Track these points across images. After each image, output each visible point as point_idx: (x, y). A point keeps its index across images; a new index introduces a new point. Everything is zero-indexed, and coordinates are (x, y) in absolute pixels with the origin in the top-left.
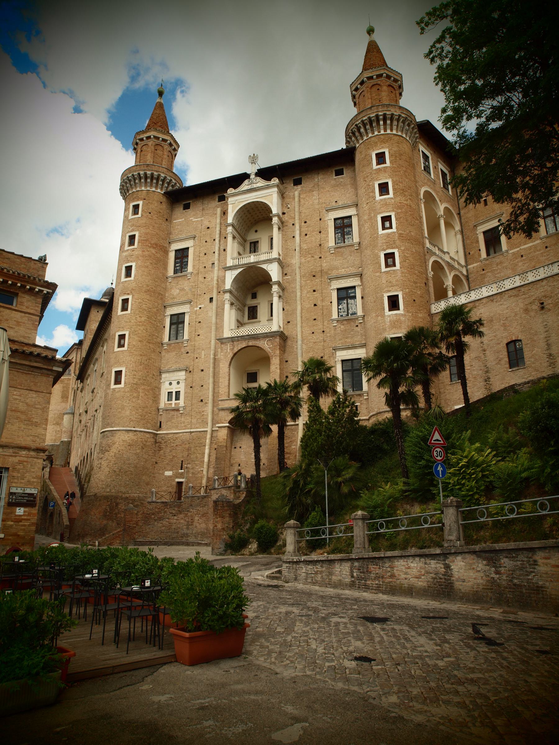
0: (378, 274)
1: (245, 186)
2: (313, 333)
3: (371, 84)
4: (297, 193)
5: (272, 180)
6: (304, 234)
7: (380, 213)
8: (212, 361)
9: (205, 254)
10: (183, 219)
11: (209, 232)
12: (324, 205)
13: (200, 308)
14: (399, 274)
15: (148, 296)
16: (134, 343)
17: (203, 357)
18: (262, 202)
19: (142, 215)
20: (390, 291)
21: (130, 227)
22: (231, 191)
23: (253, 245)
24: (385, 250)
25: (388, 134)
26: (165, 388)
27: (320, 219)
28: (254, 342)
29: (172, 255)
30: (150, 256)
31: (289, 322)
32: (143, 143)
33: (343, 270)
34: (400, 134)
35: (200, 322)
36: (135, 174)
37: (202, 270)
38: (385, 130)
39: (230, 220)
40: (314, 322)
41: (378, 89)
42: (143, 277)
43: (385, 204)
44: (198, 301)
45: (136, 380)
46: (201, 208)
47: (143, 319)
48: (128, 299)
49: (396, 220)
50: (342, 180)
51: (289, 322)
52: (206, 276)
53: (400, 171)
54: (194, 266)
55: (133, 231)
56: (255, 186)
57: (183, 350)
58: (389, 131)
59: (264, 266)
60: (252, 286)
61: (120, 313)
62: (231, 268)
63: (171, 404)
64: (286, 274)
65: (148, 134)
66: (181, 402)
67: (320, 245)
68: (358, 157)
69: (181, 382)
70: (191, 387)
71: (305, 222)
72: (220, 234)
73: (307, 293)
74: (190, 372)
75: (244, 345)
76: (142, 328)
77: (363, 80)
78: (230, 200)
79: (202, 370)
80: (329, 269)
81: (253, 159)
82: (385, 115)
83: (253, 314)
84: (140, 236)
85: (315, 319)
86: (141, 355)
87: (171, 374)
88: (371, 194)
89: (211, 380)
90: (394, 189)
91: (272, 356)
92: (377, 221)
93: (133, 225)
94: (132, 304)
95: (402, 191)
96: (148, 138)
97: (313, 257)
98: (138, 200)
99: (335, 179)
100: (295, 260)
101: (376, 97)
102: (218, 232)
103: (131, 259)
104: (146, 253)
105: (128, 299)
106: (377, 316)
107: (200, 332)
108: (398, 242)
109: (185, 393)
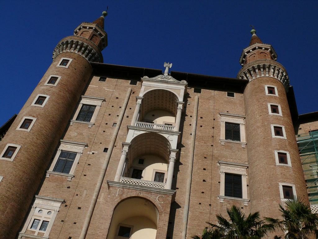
0: (272, 166)
2: (200, 204)
3: (261, 52)
4: (196, 97)
5: (182, 81)
7: (272, 123)
8: (93, 202)
13: (93, 153)
14: (291, 172)
15: (51, 126)
16: (21, 158)
17: (84, 195)
20: (285, 182)
21: (55, 72)
24: (279, 150)
26: (34, 214)
27: (214, 119)
28: (145, 194)
32: (84, 29)
33: (232, 160)
35: (90, 165)
36: (74, 40)
39: (141, 95)
40: (202, 194)
41: (265, 56)
43: (277, 119)
44: (93, 147)
45: (9, 193)
46: (115, 84)
47: (39, 142)
48: (32, 120)
49: (286, 132)
50: (232, 100)
52: (106, 130)
54: (96, 120)
55: (57, 74)
56: (167, 80)
57: (64, 184)
59: (166, 136)
60: (146, 151)
61: (18, 128)
62: (134, 128)
63: (34, 232)
66: (46, 233)
67: (213, 137)
68: (249, 87)
69: (53, 212)
70: (62, 221)
71: (201, 118)
74: (66, 206)
75: (134, 194)
76: (34, 149)
77: (255, 48)
78: (144, 83)
79: (79, 208)
80: (219, 156)
84: (61, 80)
85: (203, 193)
86: (24, 172)
87: (45, 202)
88: (265, 110)
89: (87, 219)
91: (162, 212)
92: (270, 128)
96: (90, 28)
97: (205, 143)
98: (69, 57)
99: (227, 98)
100: (189, 142)
103: (47, 93)
105: (32, 120)
106: (272, 200)
107: (87, 173)
108: (288, 147)
109: (54, 225)
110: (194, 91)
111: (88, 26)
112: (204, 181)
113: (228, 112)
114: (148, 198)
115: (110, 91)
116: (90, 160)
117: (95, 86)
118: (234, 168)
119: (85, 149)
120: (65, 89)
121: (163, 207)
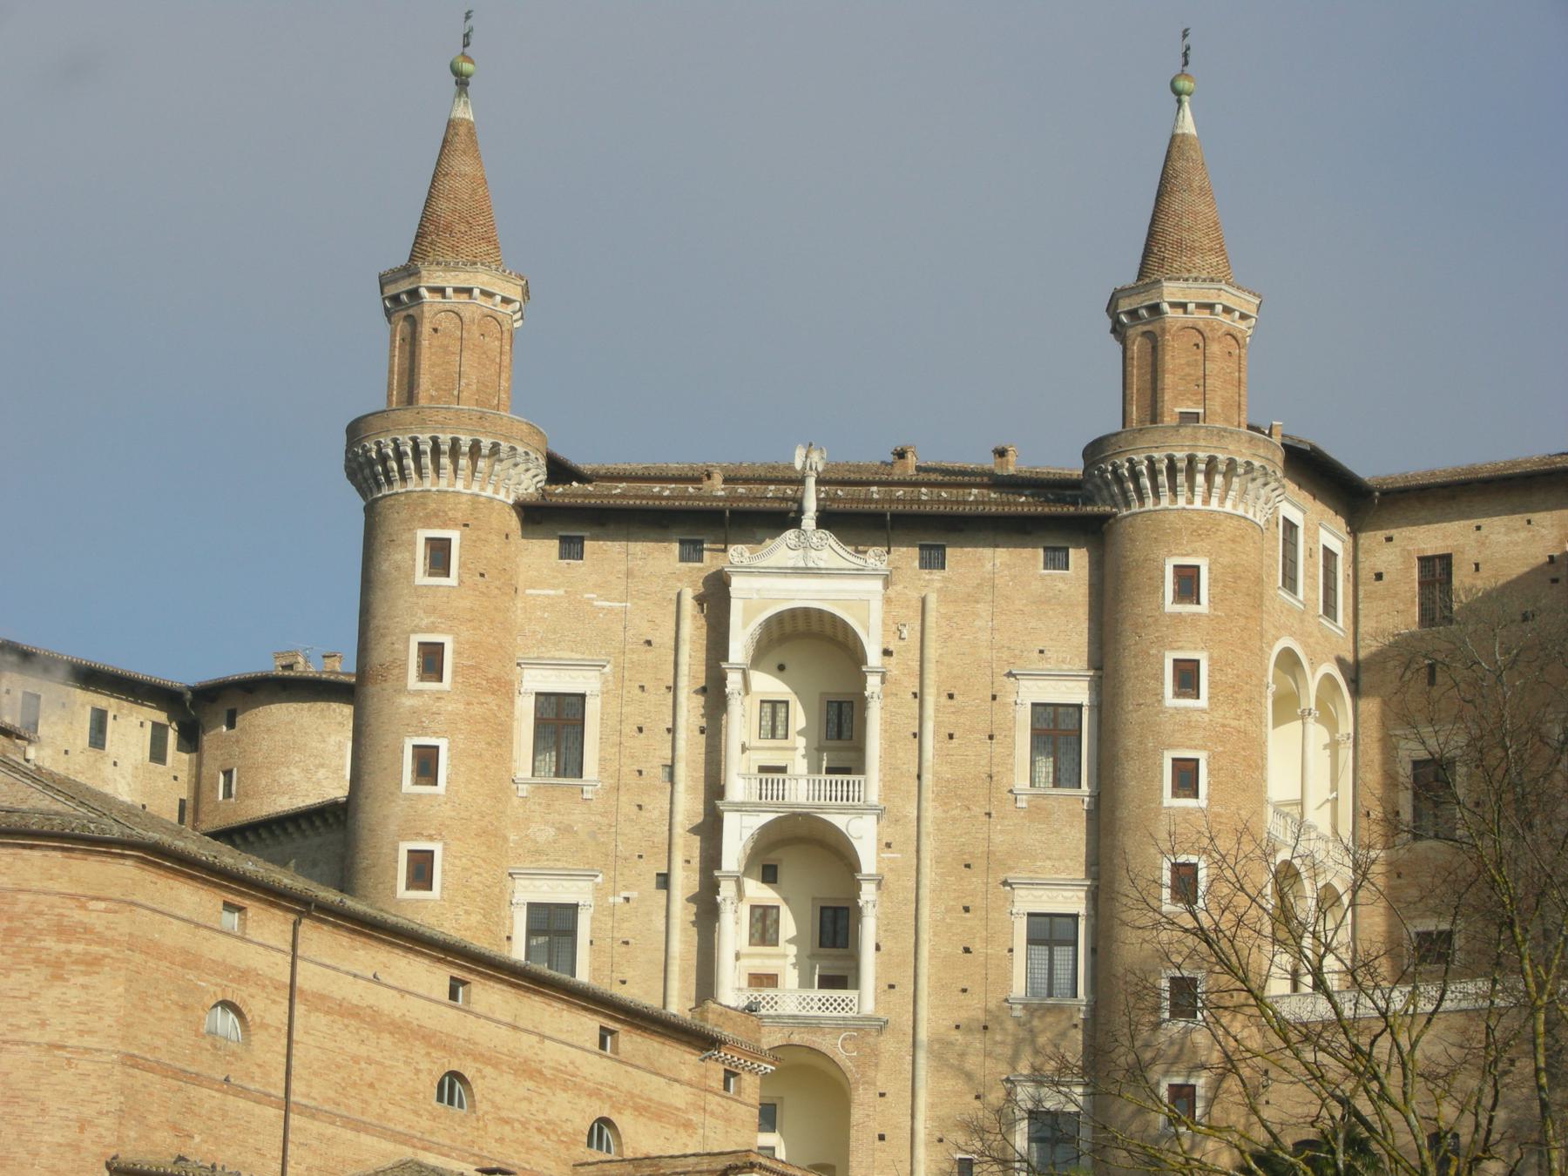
1: (782, 549)
6: (945, 731)
7: (1171, 747)
9: (640, 730)
10: (561, 592)
11: (650, 656)
12: (1005, 655)
13: (627, 899)
18: (833, 616)
19: (461, 582)
21: (420, 613)
22: (738, 553)
23: (768, 708)
25: (1213, 512)
27: (994, 698)
28: (806, 1037)
29: (525, 710)
30: (486, 720)
31: (892, 987)
33: (1049, 863)
34: (1240, 512)
35: (627, 943)
37: (632, 779)
38: (1206, 501)
40: (962, 996)
42: (471, 787)
44: (619, 878)
46: (623, 568)
49: (1209, 773)
50: (1061, 585)
51: (892, 987)
52: (645, 800)
53: (1230, 630)
54: (602, 760)
58: (1214, 504)
59: (839, 821)
64: (888, 845)
65: (462, 280)
73: (948, 910)
82: (1212, 461)
83: (764, 931)
84: (457, 653)
85: (964, 991)
90: (1212, 684)
91: (857, 1082)
93: (432, 610)
94: (444, 871)
95: (1229, 691)
98: (444, 526)
99: (1042, 578)
101: (1187, 370)
104: (477, 710)
110: (917, 564)
111: (450, 280)
112: (967, 950)
113: (1041, 652)
114: (816, 1046)
115: (611, 610)
116: (625, 925)
117: (552, 592)
118: (1055, 893)
119: (597, 888)
120: (477, 685)
121: (858, 1066)
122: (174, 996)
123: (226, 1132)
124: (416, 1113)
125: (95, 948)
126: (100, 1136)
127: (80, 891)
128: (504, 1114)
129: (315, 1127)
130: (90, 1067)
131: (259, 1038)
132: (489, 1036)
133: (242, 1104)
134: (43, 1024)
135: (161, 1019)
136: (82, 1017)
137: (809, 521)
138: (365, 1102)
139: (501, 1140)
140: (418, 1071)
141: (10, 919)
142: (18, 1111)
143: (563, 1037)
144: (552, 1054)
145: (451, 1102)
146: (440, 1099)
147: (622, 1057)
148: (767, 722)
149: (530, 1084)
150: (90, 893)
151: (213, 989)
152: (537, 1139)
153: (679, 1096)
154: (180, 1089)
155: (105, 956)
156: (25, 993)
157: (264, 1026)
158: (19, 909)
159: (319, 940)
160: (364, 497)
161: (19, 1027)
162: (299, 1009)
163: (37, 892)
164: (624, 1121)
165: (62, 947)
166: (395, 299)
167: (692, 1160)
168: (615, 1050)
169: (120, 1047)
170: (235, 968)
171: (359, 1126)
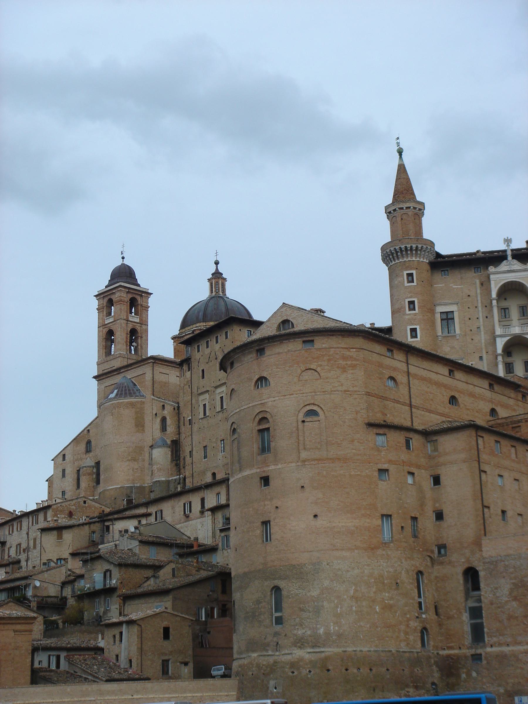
1: (504, 266)
10: (443, 285)
19: (417, 284)
22: (491, 269)
23: (503, 310)
29: (438, 317)
54: (461, 328)
55: (410, 297)
65: (408, 205)
72: (482, 302)
81: (508, 241)
83: (510, 370)
84: (418, 303)
93: (410, 292)
98: (411, 269)
102: (480, 301)
122: (377, 375)
123: (396, 414)
124: (445, 408)
125: (354, 362)
126: (362, 415)
127: (348, 347)
128: (467, 407)
129: (419, 412)
130: (357, 396)
131: (401, 387)
132: (461, 386)
133: (399, 405)
134: (342, 385)
135: (374, 382)
136: (353, 382)
137: (510, 258)
138: (431, 404)
139: (467, 415)
140: (443, 396)
141: (329, 356)
142: (338, 410)
143: (480, 386)
144: (478, 390)
145: (453, 405)
146: (450, 404)
147: (496, 391)
148: (503, 314)
149: (473, 399)
150: (351, 347)
151: (387, 373)
152: (477, 414)
153: (511, 402)
154: (382, 402)
155: (357, 364)
156: (335, 377)
157: (402, 383)
158: (331, 353)
159: (413, 360)
160: (387, 265)
161: (336, 387)
162: (411, 379)
163: (335, 348)
164: (498, 409)
165: (345, 362)
166: (390, 212)
167: (523, 416)
168: (493, 389)
169: (366, 390)
170: (392, 367)
171: (430, 411)
